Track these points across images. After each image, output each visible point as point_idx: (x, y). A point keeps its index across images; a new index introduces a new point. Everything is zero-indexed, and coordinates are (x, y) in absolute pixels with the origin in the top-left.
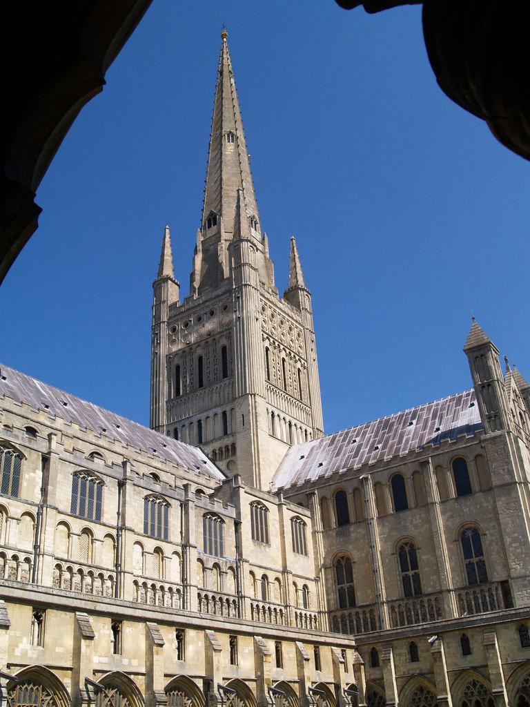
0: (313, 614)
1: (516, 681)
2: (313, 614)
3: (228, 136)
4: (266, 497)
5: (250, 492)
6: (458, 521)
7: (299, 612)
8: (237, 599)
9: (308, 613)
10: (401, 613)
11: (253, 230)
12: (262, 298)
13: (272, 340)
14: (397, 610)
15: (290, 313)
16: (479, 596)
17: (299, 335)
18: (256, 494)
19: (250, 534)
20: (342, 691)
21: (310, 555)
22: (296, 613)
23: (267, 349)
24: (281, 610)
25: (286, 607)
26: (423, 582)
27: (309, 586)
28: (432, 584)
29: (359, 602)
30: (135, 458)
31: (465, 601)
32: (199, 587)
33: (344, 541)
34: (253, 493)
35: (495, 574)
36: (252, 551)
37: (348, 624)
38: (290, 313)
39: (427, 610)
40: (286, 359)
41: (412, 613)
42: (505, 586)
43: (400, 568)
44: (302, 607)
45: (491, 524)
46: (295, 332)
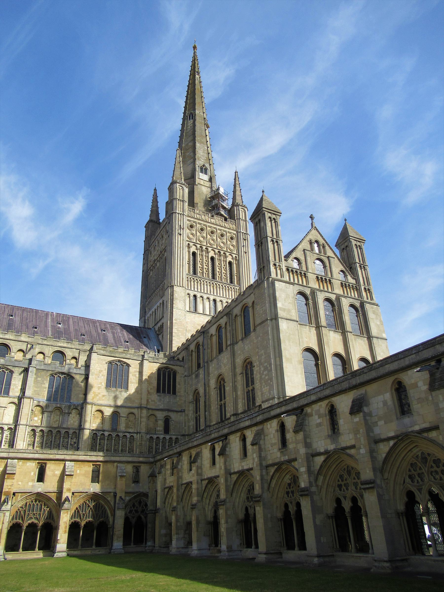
0: (174, 437)
2: (174, 437)
4: (128, 356)
5: (109, 354)
6: (242, 357)
7: (155, 437)
8: (77, 431)
11: (201, 174)
12: (190, 219)
13: (198, 246)
17: (232, 238)
18: (117, 355)
19: (104, 384)
20: (118, 498)
21: (177, 394)
23: (194, 254)
25: (137, 433)
30: (40, 342)
32: (37, 425)
33: (197, 381)
34: (113, 355)
35: (258, 399)
36: (104, 396)
40: (216, 257)
44: (163, 433)
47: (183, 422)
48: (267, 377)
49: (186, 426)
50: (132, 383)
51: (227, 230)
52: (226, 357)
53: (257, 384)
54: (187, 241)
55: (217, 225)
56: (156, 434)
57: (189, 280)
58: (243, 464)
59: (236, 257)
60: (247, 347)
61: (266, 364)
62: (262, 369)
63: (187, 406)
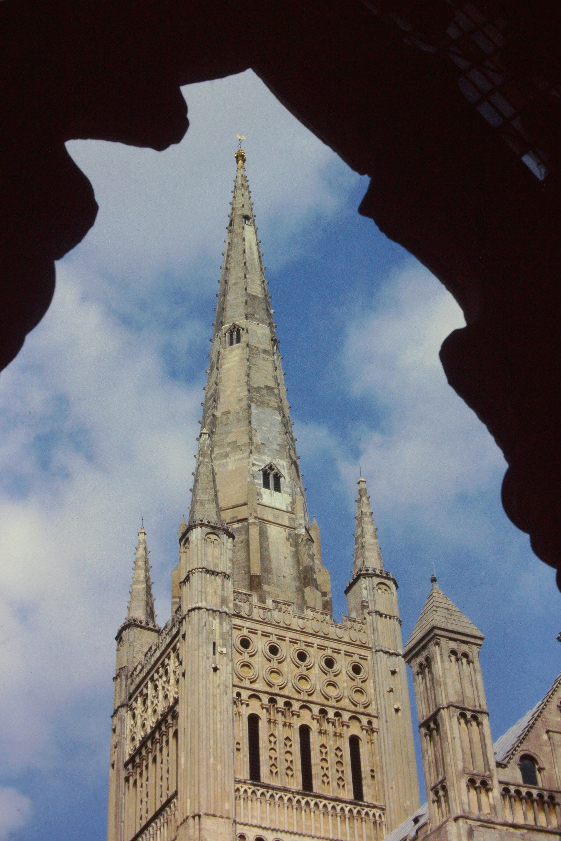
3: (231, 335)
11: (263, 490)
13: (265, 699)
15: (334, 632)
17: (357, 669)
23: (253, 720)
38: (334, 632)
51: (343, 648)
54: (234, 686)
55: (315, 635)
59: (370, 723)
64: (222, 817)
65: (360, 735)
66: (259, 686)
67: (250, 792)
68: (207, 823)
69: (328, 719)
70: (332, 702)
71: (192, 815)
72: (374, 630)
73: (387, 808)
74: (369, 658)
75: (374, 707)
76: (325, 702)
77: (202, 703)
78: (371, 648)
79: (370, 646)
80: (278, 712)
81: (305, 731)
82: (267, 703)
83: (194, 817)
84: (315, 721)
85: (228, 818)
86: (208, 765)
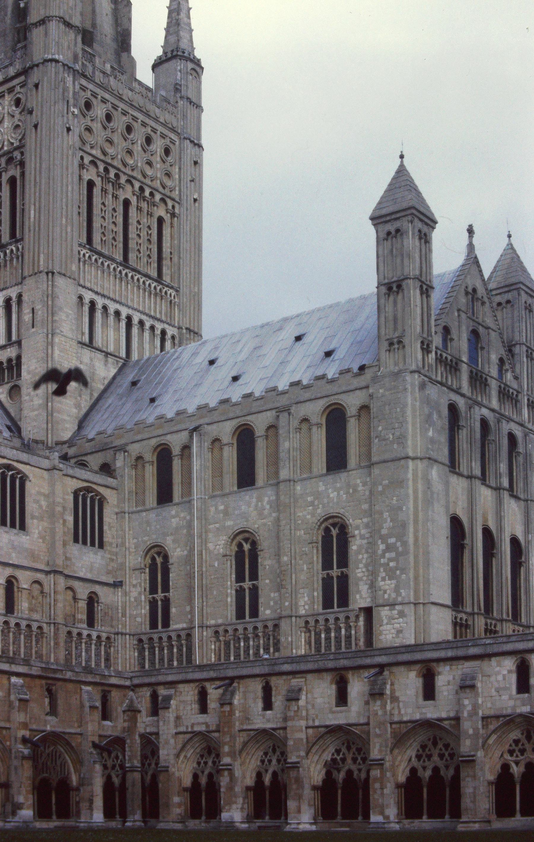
0: (104, 636)
1: (324, 750)
2: (104, 636)
7: (75, 631)
9: (94, 635)
10: (227, 644)
14: (221, 638)
16: (332, 627)
22: (69, 633)
24: (40, 628)
26: (261, 600)
27: (100, 594)
28: (272, 603)
29: (174, 626)
31: (313, 633)
35: (358, 596)
37: (157, 652)
39: (261, 642)
40: (134, 200)
41: (242, 644)
42: (368, 612)
43: (234, 576)
44: (85, 626)
45: (365, 520)
46: (158, 145)
47: (120, 608)
48: (392, 564)
49: (125, 616)
50: (33, 517)
52: (266, 499)
53: (357, 571)
56: (77, 628)
57: (142, 287)
58: (424, 710)
60: (336, 493)
61: (392, 540)
62: (382, 547)
63: (127, 576)
64: (70, 278)
65: (165, 218)
66: (97, 152)
67: (87, 255)
68: (60, 281)
69: (108, 178)
70: (128, 171)
71: (46, 271)
72: (184, 117)
73: (181, 291)
74: (177, 143)
75: (177, 193)
76: (123, 169)
77: (57, 162)
78: (179, 134)
79: (179, 131)
80: (109, 182)
81: (127, 203)
82: (102, 171)
83: (47, 273)
84: (135, 197)
85: (74, 279)
86: (61, 224)
